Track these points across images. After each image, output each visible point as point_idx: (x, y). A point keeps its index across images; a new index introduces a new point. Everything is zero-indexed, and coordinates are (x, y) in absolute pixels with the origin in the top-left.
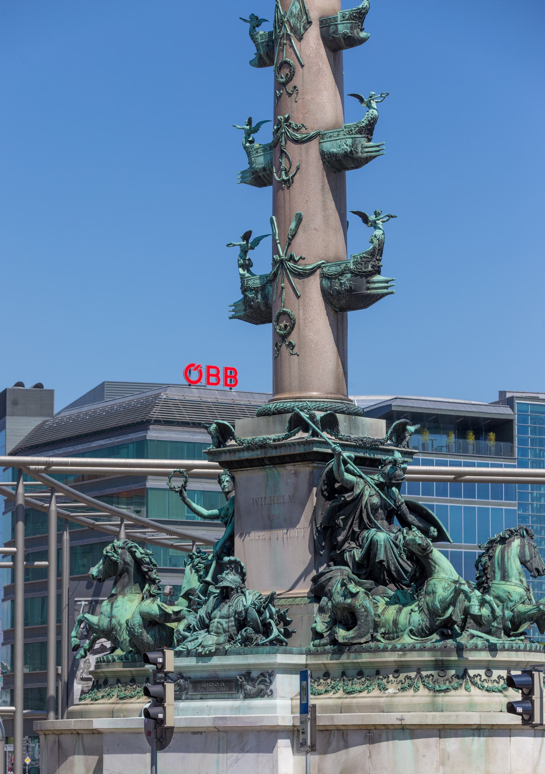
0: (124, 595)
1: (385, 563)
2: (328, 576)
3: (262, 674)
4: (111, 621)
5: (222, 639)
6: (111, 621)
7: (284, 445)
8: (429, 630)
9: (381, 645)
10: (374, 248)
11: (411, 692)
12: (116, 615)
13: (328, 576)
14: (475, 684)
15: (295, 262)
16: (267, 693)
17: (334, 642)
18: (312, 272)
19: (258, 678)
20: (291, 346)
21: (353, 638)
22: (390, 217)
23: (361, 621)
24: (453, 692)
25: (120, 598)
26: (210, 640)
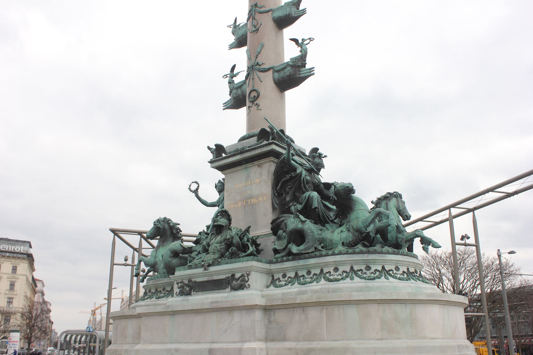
1: (317, 210)
2: (282, 219)
3: (242, 276)
5: (216, 256)
8: (354, 243)
9: (324, 253)
10: (302, 55)
11: (348, 280)
13: (282, 219)
14: (391, 276)
15: (260, 65)
16: (245, 286)
17: (290, 253)
18: (269, 69)
19: (239, 278)
22: (311, 39)
23: (309, 238)
24: (378, 280)
26: (209, 258)
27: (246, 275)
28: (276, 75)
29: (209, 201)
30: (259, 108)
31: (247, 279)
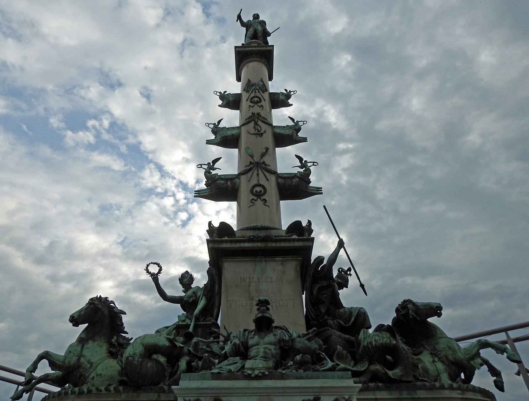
0: (94, 341)
4: (79, 359)
5: (271, 364)
6: (79, 359)
12: (86, 354)
15: (266, 165)
20: (265, 200)
28: (280, 180)
29: (169, 292)
30: (267, 204)
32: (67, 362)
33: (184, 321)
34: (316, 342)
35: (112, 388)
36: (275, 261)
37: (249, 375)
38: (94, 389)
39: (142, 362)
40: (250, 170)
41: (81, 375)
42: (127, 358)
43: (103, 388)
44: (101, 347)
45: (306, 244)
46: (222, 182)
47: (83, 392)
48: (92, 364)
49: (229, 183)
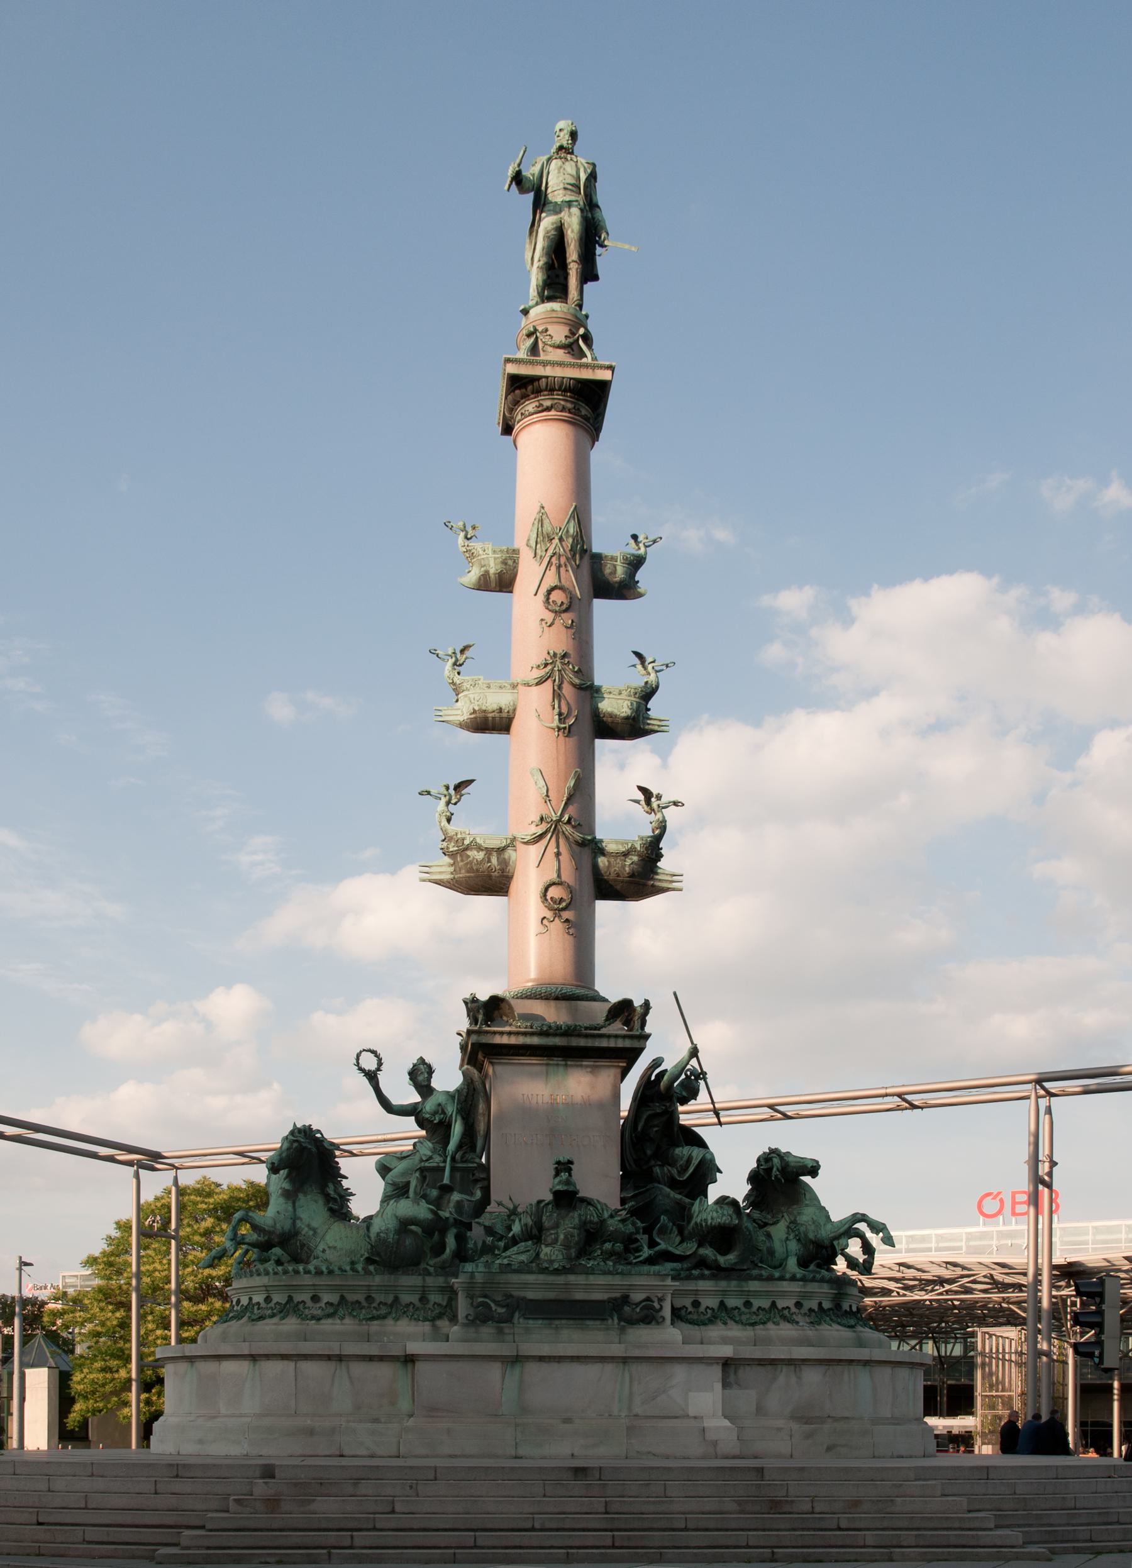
0: (305, 1194)
4: (294, 1223)
5: (573, 1252)
7: (601, 1036)
21: (736, 1263)
25: (301, 1196)
27: (656, 1300)
29: (395, 1101)
31: (656, 1305)
32: (278, 1226)
33: (431, 1158)
34: (634, 1224)
35: (359, 1267)
36: (581, 1066)
37: (547, 1268)
38: (336, 1269)
39: (399, 1240)
40: (541, 836)
41: (303, 1245)
42: (378, 1234)
43: (348, 1268)
44: (316, 1202)
45: (636, 1044)
46: (480, 856)
47: (321, 1273)
48: (315, 1230)
49: (494, 860)
